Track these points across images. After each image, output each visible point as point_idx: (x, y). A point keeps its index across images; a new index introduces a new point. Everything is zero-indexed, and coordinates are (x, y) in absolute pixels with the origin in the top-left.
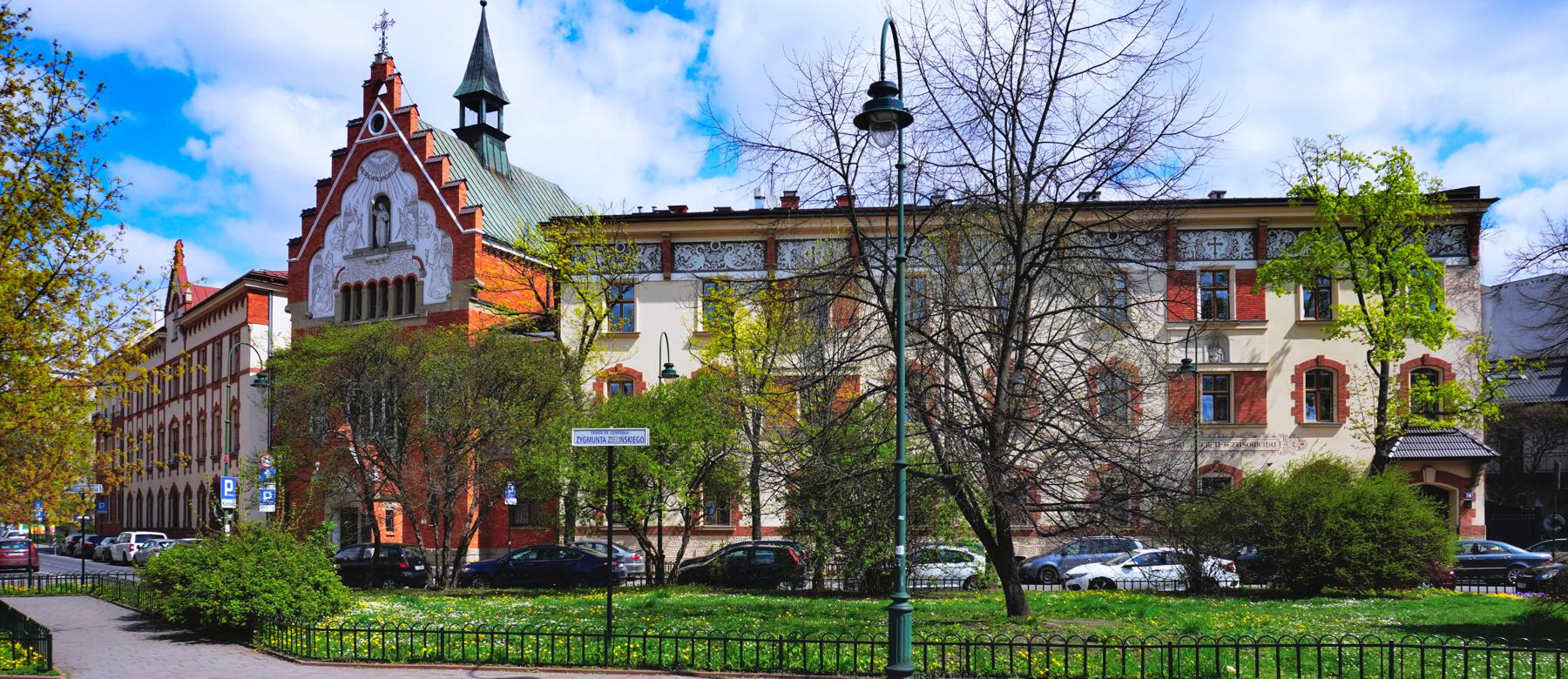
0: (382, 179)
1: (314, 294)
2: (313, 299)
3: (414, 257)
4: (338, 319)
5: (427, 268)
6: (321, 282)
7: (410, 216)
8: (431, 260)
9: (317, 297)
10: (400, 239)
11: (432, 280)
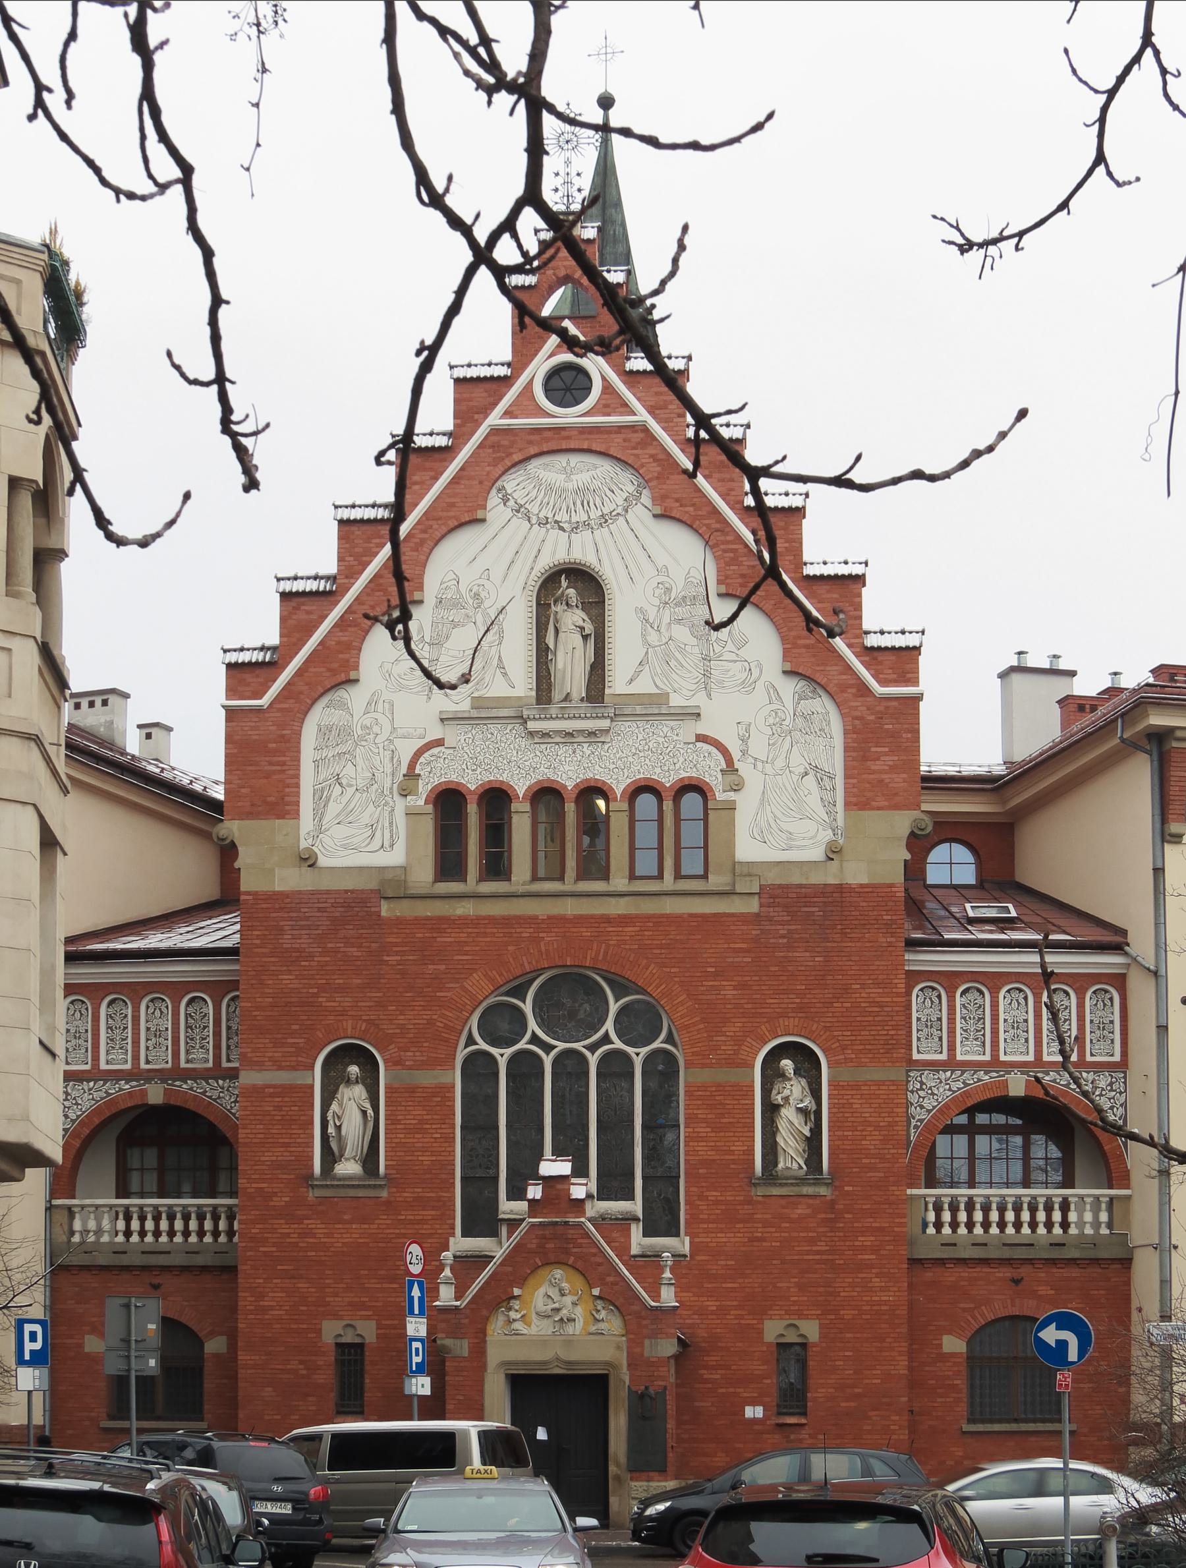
1: (322, 799)
2: (319, 815)
4: (423, 874)
9: (333, 809)
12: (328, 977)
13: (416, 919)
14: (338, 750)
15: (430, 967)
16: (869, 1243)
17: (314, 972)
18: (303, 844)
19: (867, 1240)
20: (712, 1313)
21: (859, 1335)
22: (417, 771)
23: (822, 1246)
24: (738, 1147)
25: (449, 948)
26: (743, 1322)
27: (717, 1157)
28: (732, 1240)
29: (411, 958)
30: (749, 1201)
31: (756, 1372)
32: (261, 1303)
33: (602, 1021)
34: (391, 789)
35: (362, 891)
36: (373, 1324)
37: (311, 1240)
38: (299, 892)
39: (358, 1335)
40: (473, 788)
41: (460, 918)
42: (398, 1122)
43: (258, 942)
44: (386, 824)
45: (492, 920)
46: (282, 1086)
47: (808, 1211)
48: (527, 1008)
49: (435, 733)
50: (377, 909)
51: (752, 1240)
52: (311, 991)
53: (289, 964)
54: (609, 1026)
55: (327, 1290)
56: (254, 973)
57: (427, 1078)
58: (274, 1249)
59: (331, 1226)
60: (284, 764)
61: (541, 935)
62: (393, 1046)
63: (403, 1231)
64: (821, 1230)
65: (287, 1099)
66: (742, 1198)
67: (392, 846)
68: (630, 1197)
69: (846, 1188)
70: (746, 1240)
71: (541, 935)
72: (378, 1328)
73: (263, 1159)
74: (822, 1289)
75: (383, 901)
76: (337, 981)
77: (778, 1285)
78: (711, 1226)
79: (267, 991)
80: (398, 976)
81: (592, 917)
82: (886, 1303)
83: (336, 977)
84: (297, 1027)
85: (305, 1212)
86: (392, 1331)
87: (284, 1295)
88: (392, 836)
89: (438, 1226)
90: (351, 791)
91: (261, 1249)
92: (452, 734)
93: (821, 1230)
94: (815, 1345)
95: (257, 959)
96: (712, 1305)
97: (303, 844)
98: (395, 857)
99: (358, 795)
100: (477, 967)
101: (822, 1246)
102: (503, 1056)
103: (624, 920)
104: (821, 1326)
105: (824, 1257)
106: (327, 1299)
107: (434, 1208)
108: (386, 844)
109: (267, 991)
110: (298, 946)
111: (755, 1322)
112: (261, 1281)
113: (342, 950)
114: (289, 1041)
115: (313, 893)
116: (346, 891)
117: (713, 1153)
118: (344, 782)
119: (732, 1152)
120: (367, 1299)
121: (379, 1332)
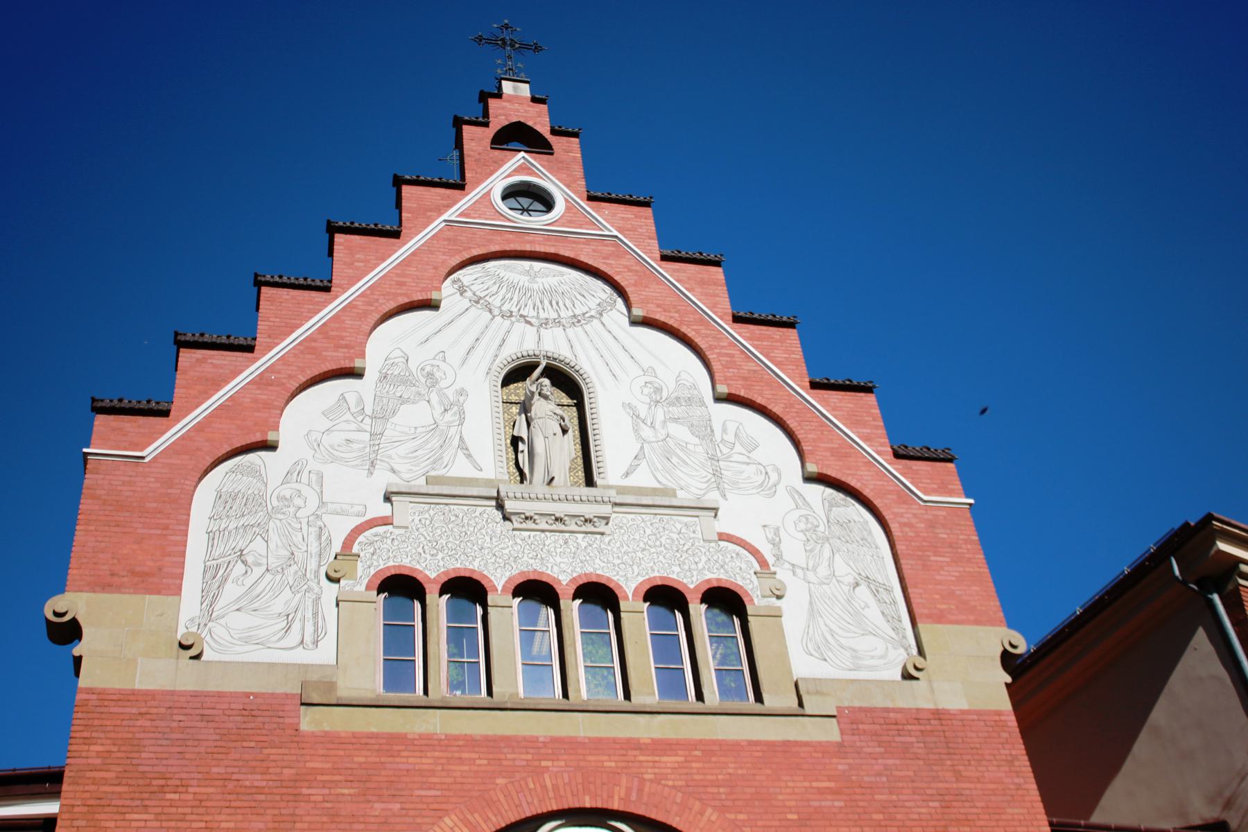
0: (545, 323)
1: (215, 575)
2: (210, 598)
3: (723, 537)
5: (783, 574)
6: (259, 545)
7: (681, 432)
8: (793, 549)
9: (231, 592)
10: (643, 478)
11: (813, 612)
12: (209, 818)
13: (354, 735)
15: (376, 805)
17: (189, 810)
22: (355, 549)
25: (405, 779)
29: (346, 791)
34: (317, 572)
38: (173, 693)
40: (433, 575)
41: (421, 736)
43: (98, 761)
44: (309, 615)
45: (471, 742)
49: (384, 510)
50: (295, 720)
53: (146, 796)
56: (85, 809)
60: (166, 528)
61: (544, 763)
71: (544, 763)
75: (303, 708)
76: (224, 825)
80: (325, 819)
81: (615, 741)
83: (223, 817)
88: (316, 630)
90: (258, 571)
92: (404, 510)
95: (92, 788)
100: (450, 807)
103: (661, 747)
108: (308, 639)
110: (163, 769)
113: (235, 777)
115: (195, 695)
116: (247, 695)
118: (250, 559)
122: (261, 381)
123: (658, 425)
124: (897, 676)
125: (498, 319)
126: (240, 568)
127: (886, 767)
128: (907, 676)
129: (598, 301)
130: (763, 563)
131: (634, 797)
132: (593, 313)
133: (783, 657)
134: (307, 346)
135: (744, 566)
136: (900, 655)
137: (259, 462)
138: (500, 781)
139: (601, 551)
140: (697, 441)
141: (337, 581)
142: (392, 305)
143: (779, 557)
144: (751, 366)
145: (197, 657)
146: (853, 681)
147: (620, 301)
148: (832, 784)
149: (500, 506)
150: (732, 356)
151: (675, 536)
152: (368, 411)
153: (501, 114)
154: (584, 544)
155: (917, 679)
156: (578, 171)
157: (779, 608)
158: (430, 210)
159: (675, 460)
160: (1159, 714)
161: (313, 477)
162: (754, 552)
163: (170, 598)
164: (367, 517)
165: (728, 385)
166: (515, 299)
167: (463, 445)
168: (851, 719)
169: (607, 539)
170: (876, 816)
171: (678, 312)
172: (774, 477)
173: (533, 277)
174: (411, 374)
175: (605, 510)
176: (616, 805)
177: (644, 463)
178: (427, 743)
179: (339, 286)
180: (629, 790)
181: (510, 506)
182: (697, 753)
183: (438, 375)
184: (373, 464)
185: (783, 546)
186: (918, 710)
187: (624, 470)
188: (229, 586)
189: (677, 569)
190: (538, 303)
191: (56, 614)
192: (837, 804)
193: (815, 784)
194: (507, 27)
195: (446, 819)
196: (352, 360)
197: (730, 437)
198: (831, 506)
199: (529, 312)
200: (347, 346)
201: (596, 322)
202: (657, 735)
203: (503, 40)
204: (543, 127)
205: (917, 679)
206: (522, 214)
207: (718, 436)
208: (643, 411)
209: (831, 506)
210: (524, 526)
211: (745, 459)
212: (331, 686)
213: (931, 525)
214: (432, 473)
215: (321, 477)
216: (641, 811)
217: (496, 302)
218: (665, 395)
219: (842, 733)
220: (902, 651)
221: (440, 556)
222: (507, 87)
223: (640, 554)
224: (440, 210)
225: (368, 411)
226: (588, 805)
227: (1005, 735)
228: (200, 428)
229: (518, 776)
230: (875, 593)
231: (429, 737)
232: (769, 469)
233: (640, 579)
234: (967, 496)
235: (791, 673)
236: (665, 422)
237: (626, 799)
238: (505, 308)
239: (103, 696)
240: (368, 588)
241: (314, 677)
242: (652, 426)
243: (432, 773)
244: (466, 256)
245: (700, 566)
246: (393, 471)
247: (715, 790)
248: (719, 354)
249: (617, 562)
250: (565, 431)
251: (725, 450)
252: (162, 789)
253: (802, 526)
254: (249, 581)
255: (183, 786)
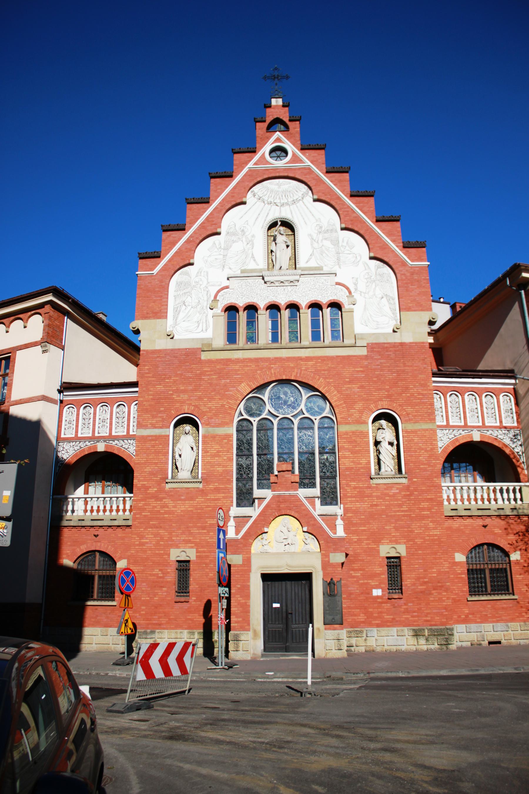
0: (283, 205)
1: (177, 311)
2: (175, 318)
3: (338, 284)
4: (221, 341)
5: (356, 295)
7: (327, 243)
8: (362, 286)
9: (181, 316)
10: (313, 264)
13: (217, 360)
14: (184, 291)
16: (426, 506)
18: (168, 330)
19: (425, 505)
20: (355, 542)
21: (425, 552)
22: (218, 298)
23: (405, 508)
24: (364, 461)
26: (370, 546)
27: (354, 466)
28: (363, 506)
30: (369, 487)
31: (377, 572)
32: (142, 541)
33: (299, 405)
34: (207, 306)
35: (194, 349)
36: (194, 550)
37: (166, 509)
38: (166, 350)
39: (187, 556)
40: (241, 305)
41: (236, 359)
42: (207, 452)
44: (204, 321)
45: (250, 360)
46: (156, 436)
47: (397, 491)
48: (266, 398)
49: (226, 283)
51: (372, 506)
52: (170, 392)
54: (302, 407)
55: (173, 534)
57: (221, 431)
58: (149, 514)
59: (176, 502)
60: (161, 297)
61: (272, 366)
62: (206, 417)
63: (209, 504)
64: (404, 500)
65: (157, 442)
66: (366, 485)
67: (206, 330)
68: (313, 485)
69: (415, 480)
70: (369, 506)
71: (272, 366)
72: (197, 552)
73: (145, 470)
74: (406, 529)
77: (386, 527)
78: (353, 499)
79: (150, 393)
81: (294, 358)
82: (436, 535)
84: (163, 409)
85: (164, 496)
86: (204, 554)
87: (153, 536)
89: (225, 502)
90: (189, 308)
91: (143, 514)
92: (233, 283)
93: (404, 500)
94: (404, 557)
96: (355, 538)
97: (168, 330)
98: (208, 334)
99: (192, 309)
101: (405, 508)
102: (255, 421)
103: (308, 359)
104: (407, 548)
105: (406, 513)
106: (173, 538)
107: (224, 493)
108: (204, 329)
109: (150, 393)
111: (375, 546)
112: (142, 529)
114: (159, 415)
115: (172, 350)
116: (186, 349)
117: (352, 464)
118: (187, 304)
119: (361, 464)
120: (191, 538)
121: (198, 554)
122: (188, 241)
123: (320, 241)
124: (392, 331)
125: (267, 205)
126: (184, 307)
127: (381, 363)
128: (394, 331)
129: (302, 193)
130: (350, 292)
131: (298, 375)
132: (300, 198)
133: (352, 326)
134: (202, 226)
135: (343, 294)
136: (393, 324)
137: (188, 270)
138: (258, 372)
139: (295, 292)
140: (333, 246)
141: (212, 309)
142: (230, 205)
143: (356, 289)
144: (354, 215)
145: (172, 338)
146: (374, 334)
147: (310, 192)
148: (362, 369)
149: (263, 279)
150: (348, 211)
151: (321, 284)
152: (222, 247)
153: (271, 115)
154: (290, 290)
155: (396, 332)
156: (298, 137)
157: (353, 309)
158: (243, 164)
159: (324, 255)
160: (502, 330)
161: (205, 273)
162: (347, 288)
163: (164, 320)
164: (222, 286)
165: (345, 224)
166: (273, 196)
167: (253, 257)
168: (372, 347)
169: (298, 287)
170: (374, 379)
171: (330, 195)
172: (359, 258)
173: (279, 185)
174: (236, 231)
175: (297, 278)
176: (293, 378)
177: (313, 257)
178: (237, 361)
179: (212, 200)
180: (297, 373)
181: (266, 279)
182: (320, 360)
183: (245, 230)
184: (224, 267)
185: (358, 285)
186: (395, 343)
187: (306, 261)
188: (181, 313)
189: (320, 297)
190: (281, 197)
191: (133, 328)
192: (363, 375)
193: (356, 369)
194: (276, 69)
195: (242, 384)
196: (216, 229)
197: (345, 244)
198: (378, 268)
199: (277, 201)
200: (215, 224)
201: (301, 202)
202: (307, 355)
203: (274, 76)
204: (286, 119)
205: (396, 332)
206: (276, 160)
207: (340, 244)
208: (315, 236)
209: (378, 268)
210: (271, 285)
211: (349, 252)
212: (210, 345)
213: (412, 274)
214: (243, 268)
215: (207, 273)
216: (300, 380)
217: (266, 198)
218: (323, 229)
219: (368, 352)
220: (394, 321)
221: (244, 298)
222: (274, 102)
223: (308, 292)
224: (247, 163)
225: (222, 247)
226: (284, 378)
227: (424, 350)
228: (170, 261)
229: (264, 370)
230: (388, 301)
231: (238, 359)
232: (357, 255)
233: (308, 301)
234: (428, 261)
235: (354, 331)
236: (322, 240)
237: (296, 376)
238: (269, 200)
239: (147, 351)
240: (222, 311)
241: (205, 342)
242: (318, 242)
243: (239, 370)
244: (256, 181)
245: (328, 295)
246: (230, 268)
247: (323, 372)
248: (344, 211)
249: (301, 295)
250: (288, 246)
251: (342, 249)
252: (165, 379)
253: (366, 277)
254: (187, 311)
255: (170, 378)
